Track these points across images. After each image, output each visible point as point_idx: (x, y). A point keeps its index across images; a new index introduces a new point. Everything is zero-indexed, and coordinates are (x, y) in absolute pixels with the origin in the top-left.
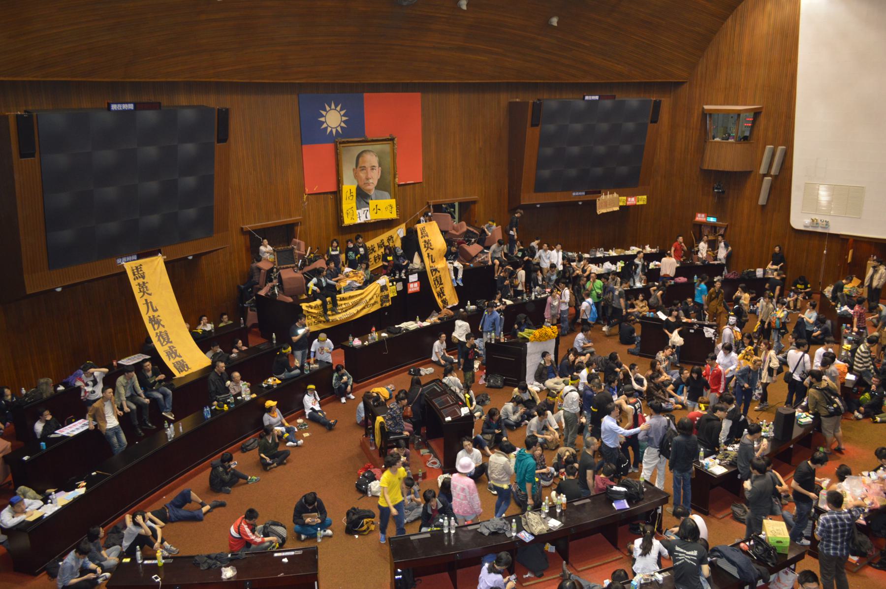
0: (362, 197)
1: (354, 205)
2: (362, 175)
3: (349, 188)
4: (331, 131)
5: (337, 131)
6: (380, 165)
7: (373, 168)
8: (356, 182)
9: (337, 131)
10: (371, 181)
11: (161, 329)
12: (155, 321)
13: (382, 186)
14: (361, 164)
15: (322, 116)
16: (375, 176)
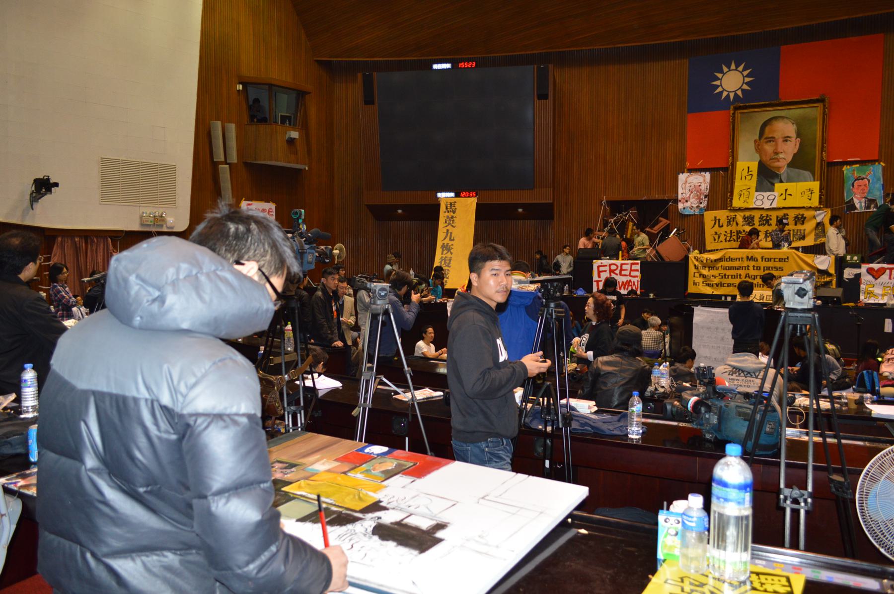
0: (767, 177)
1: (753, 183)
2: (769, 148)
3: (746, 165)
4: (728, 96)
5: (736, 95)
6: (799, 134)
7: (786, 139)
8: (757, 157)
9: (736, 95)
10: (781, 156)
11: (449, 255)
12: (447, 248)
13: (801, 162)
14: (767, 133)
15: (718, 79)
16: (789, 150)
